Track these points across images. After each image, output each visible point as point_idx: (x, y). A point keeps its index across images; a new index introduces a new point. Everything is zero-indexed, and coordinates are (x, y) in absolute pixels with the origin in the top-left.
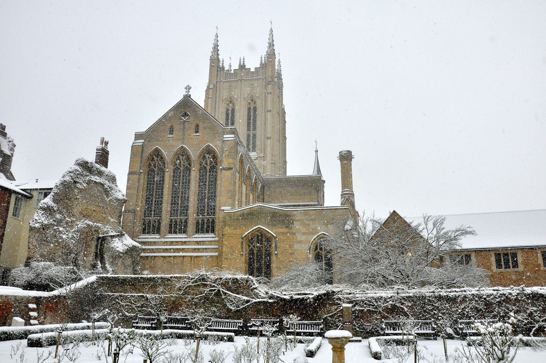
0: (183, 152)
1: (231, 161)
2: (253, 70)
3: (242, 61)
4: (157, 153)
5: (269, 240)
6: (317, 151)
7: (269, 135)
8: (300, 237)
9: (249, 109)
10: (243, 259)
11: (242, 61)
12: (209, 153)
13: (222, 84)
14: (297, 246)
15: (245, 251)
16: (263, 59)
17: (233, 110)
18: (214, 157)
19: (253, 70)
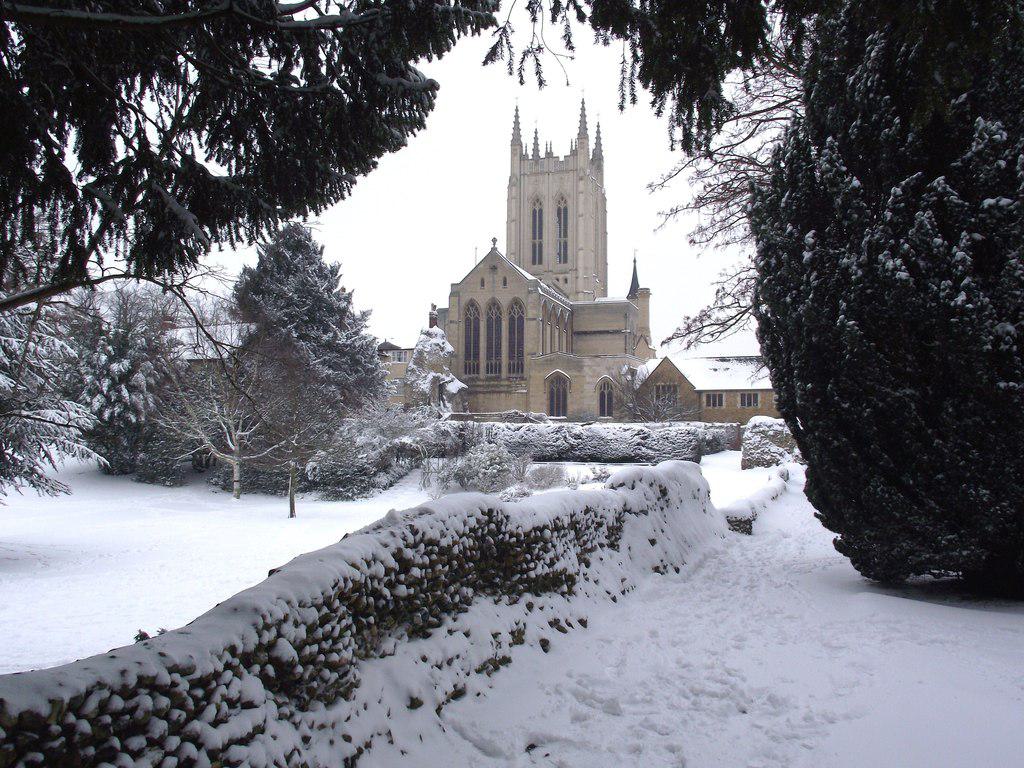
0: (494, 304)
1: (534, 312)
2: (562, 159)
3: (549, 146)
4: (472, 304)
5: (565, 382)
6: (635, 261)
7: (581, 246)
8: (588, 379)
9: (559, 210)
10: (546, 395)
11: (549, 146)
12: (516, 303)
13: (526, 177)
14: (586, 387)
15: (548, 390)
16: (574, 144)
17: (541, 211)
18: (521, 307)
19: (562, 159)
